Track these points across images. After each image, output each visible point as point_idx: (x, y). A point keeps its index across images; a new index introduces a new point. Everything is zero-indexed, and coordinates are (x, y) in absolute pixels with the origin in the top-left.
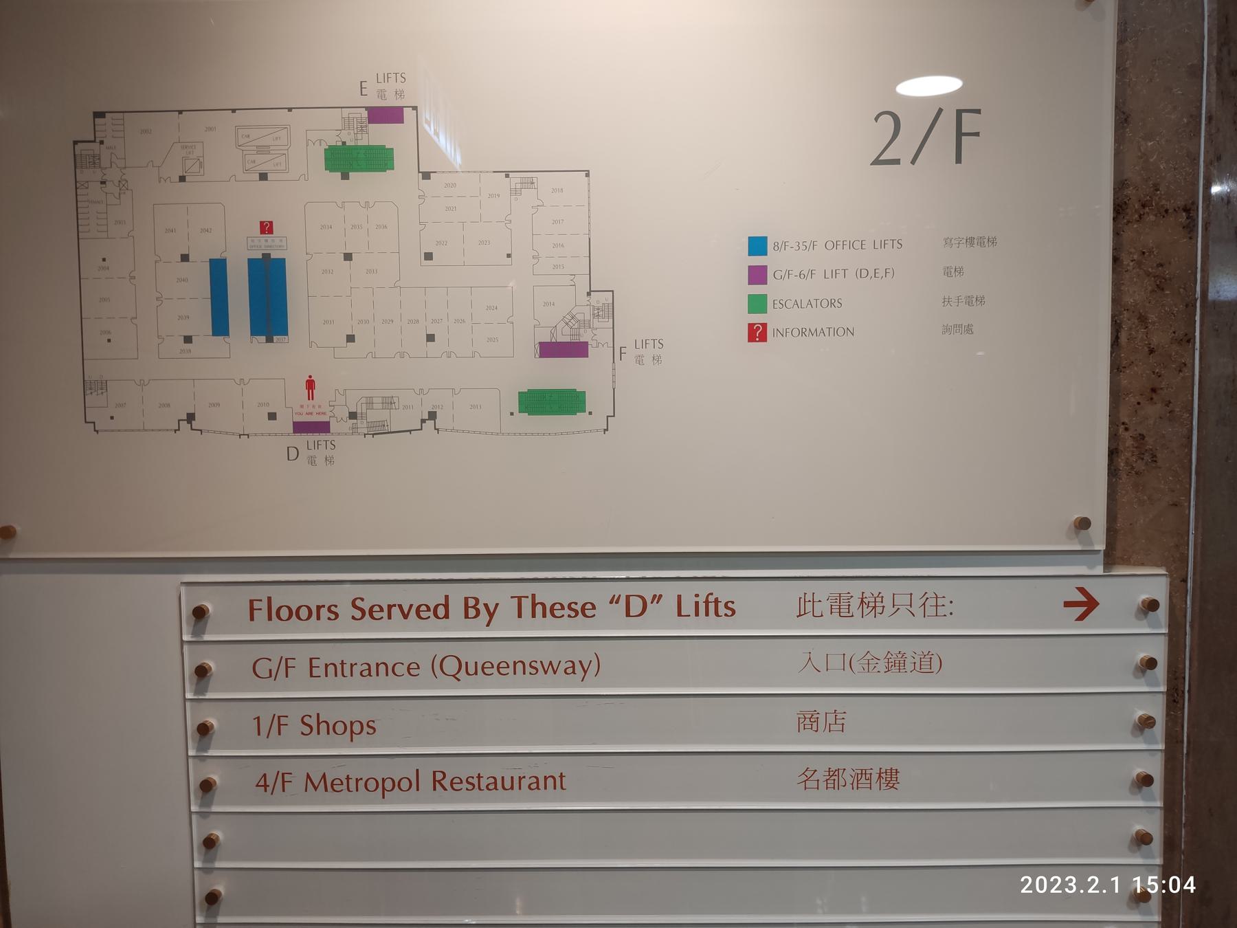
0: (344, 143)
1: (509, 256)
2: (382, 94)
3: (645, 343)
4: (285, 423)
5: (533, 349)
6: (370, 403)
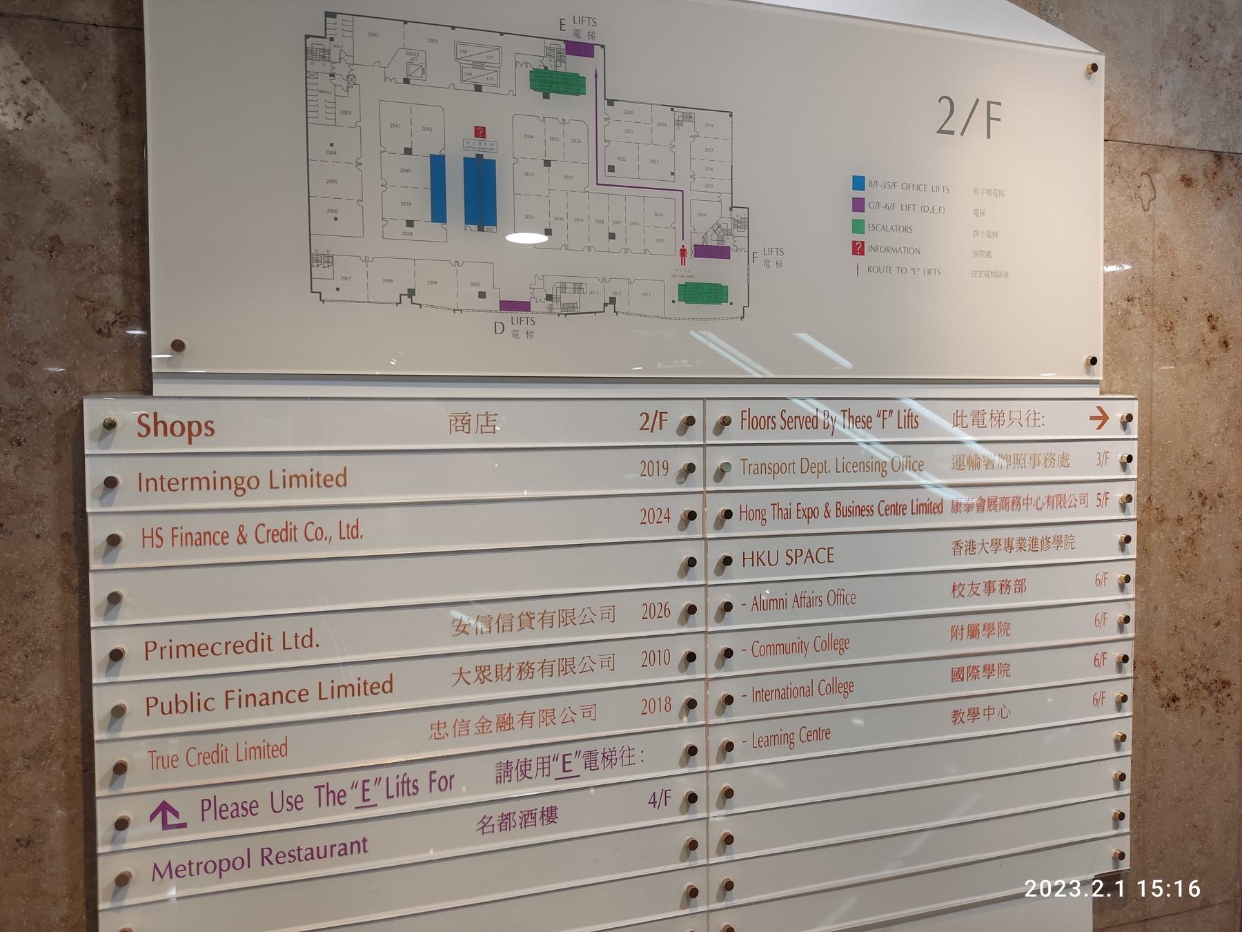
3: (771, 251)
4: (492, 302)
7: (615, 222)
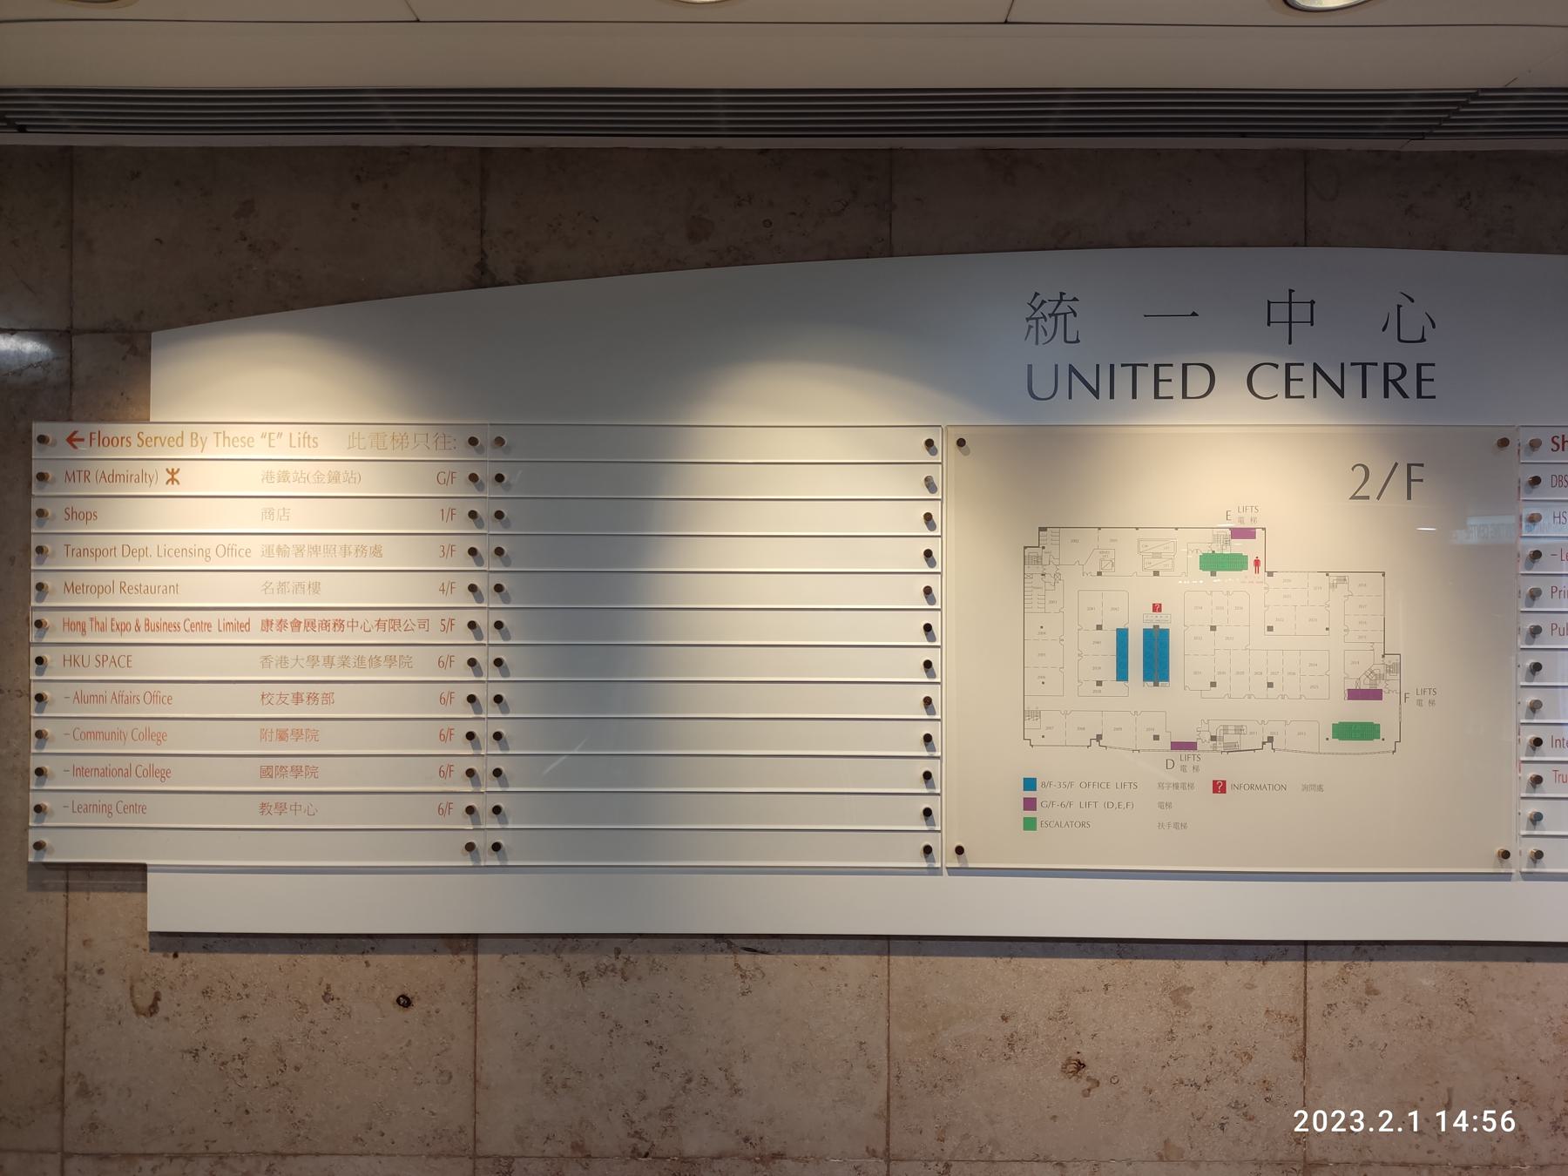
2: (1241, 520)
5: (1342, 694)
6: (1226, 730)
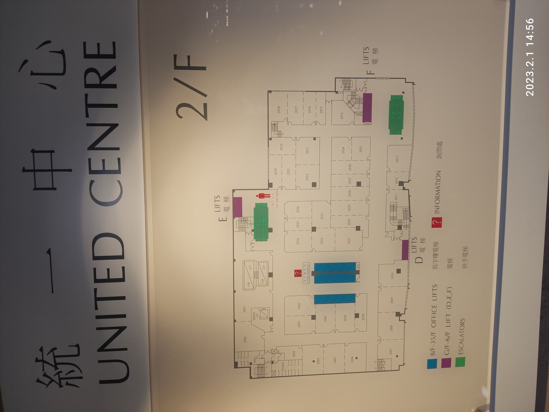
0: (253, 230)
1: (315, 139)
2: (226, 209)
7: (350, 182)
